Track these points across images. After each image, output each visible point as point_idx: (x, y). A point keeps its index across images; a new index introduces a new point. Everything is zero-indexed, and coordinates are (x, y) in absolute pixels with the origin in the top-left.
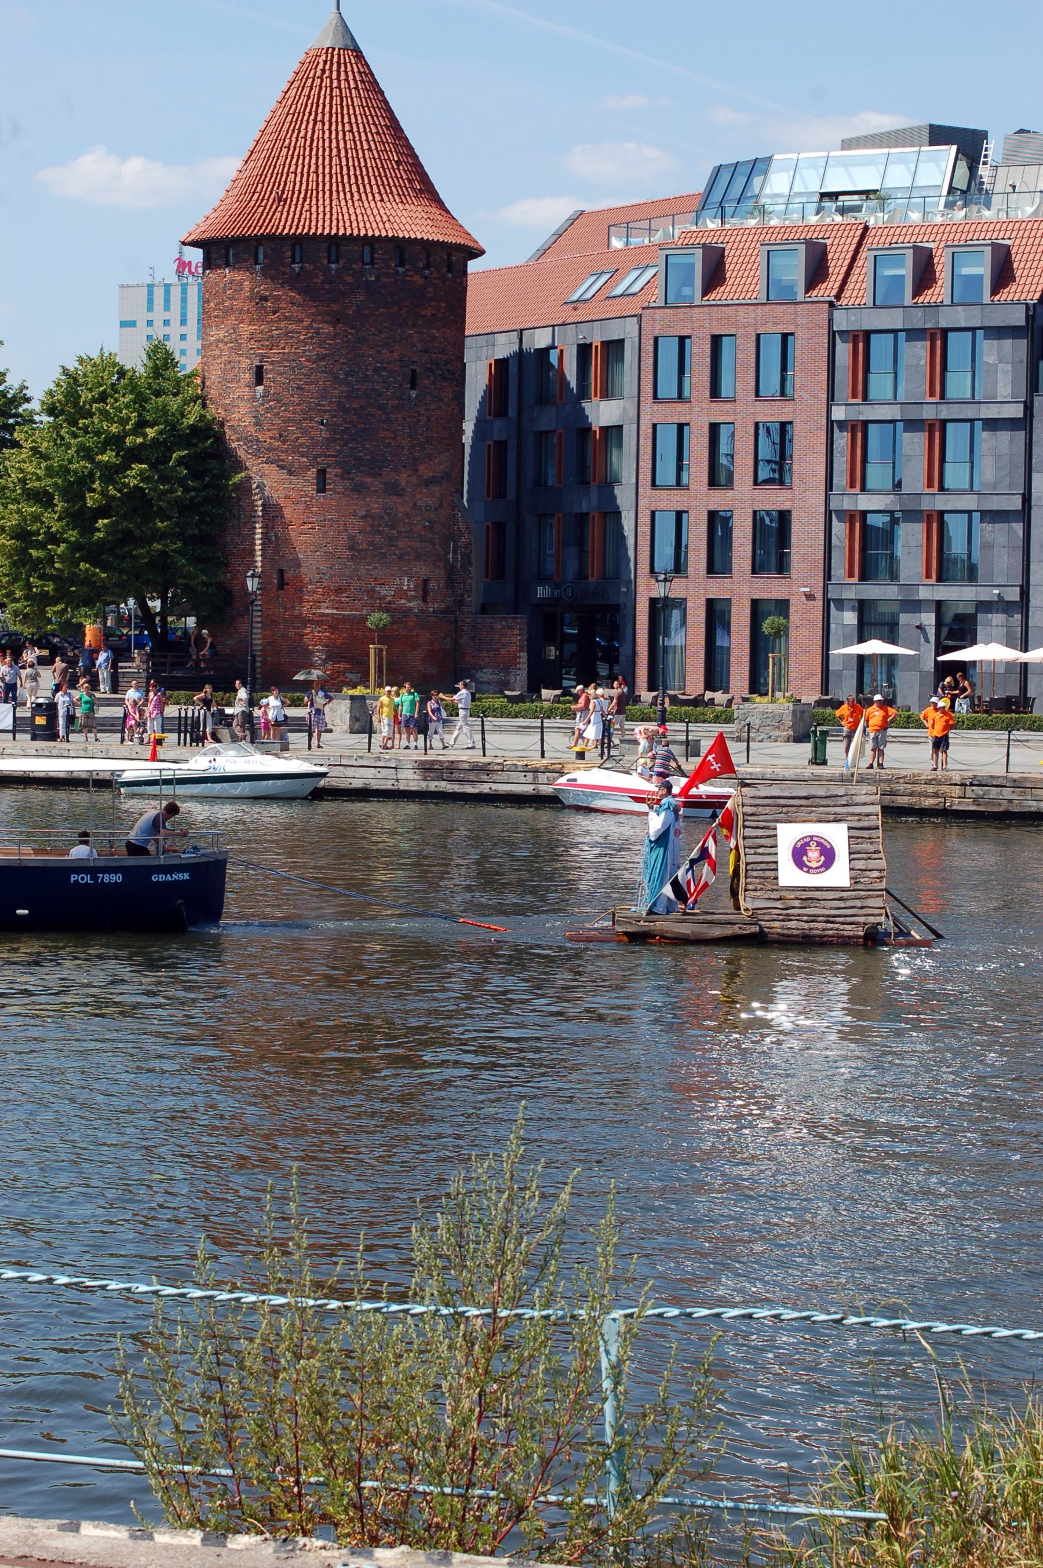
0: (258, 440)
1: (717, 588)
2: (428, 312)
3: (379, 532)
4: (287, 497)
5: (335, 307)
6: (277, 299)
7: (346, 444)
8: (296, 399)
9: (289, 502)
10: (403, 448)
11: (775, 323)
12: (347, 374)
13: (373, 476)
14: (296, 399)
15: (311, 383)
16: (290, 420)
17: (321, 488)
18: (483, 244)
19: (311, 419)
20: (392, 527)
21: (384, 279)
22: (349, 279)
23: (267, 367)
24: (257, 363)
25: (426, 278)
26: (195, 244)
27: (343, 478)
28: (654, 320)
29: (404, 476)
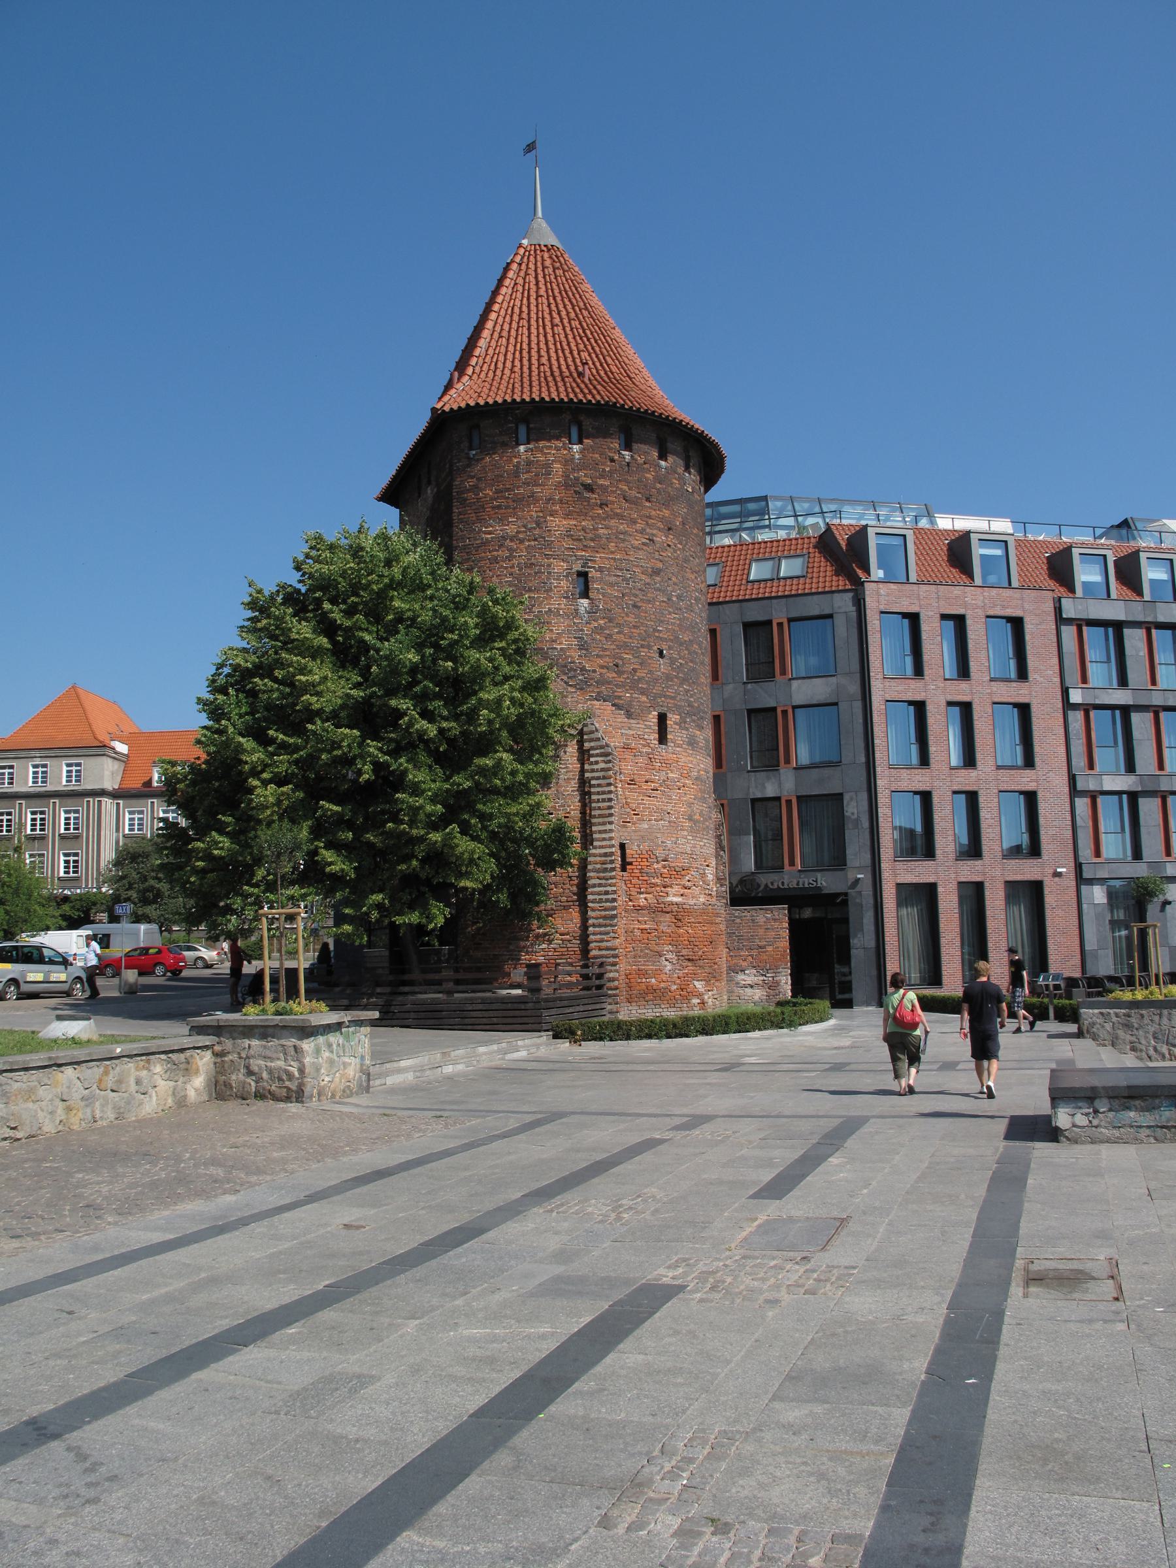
0: (583, 669)
1: (970, 871)
4: (627, 747)
5: (667, 513)
6: (604, 489)
7: (681, 684)
8: (631, 619)
9: (628, 755)
11: (1004, 607)
12: (679, 597)
14: (631, 619)
15: (649, 601)
16: (625, 646)
17: (663, 739)
19: (649, 647)
23: (593, 573)
24: (577, 567)
27: (679, 724)
28: (879, 594)
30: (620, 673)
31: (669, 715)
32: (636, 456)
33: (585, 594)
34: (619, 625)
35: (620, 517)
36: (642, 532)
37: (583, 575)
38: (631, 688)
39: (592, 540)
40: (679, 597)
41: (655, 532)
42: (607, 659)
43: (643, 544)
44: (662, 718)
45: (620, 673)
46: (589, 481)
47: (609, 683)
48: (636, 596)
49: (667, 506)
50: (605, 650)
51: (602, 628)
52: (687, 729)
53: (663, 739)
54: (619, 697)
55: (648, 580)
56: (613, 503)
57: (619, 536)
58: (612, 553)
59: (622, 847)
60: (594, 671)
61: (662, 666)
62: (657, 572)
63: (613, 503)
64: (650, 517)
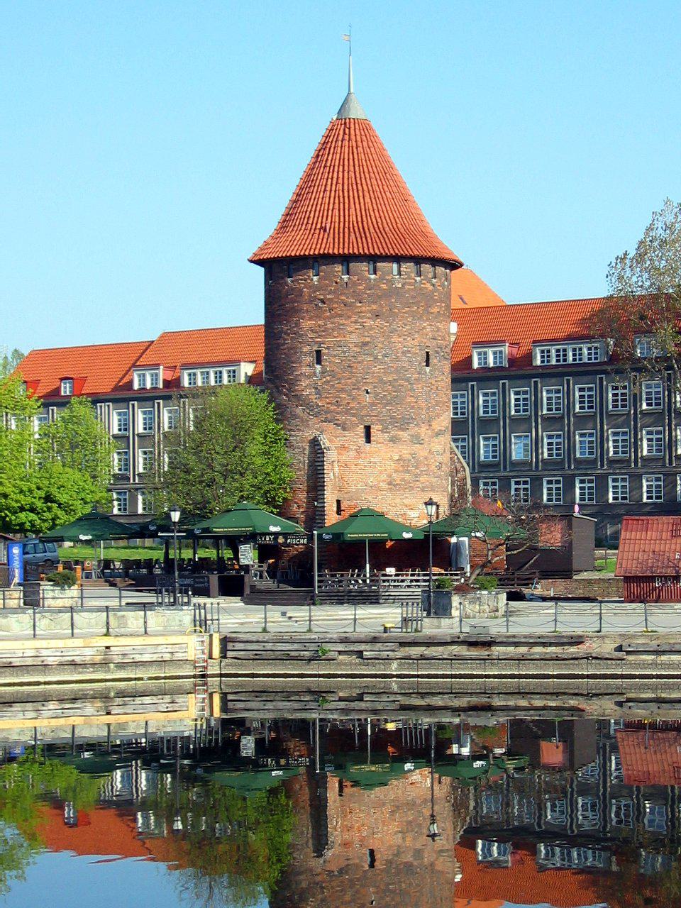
0: (318, 405)
2: (435, 310)
3: (408, 471)
5: (374, 307)
10: (422, 409)
13: (403, 430)
16: (343, 390)
17: (368, 440)
18: (462, 259)
19: (359, 389)
20: (417, 468)
21: (407, 287)
22: (384, 286)
23: (324, 351)
24: (315, 348)
25: (434, 285)
26: (259, 262)
29: (423, 429)
30: (338, 406)
31: (372, 426)
32: (351, 277)
33: (319, 362)
34: (339, 379)
35: (340, 316)
36: (356, 322)
37: (318, 352)
38: (346, 414)
39: (323, 331)
40: (384, 356)
41: (365, 320)
42: (331, 399)
43: (356, 329)
44: (368, 429)
45: (338, 406)
46: (322, 297)
47: (332, 412)
48: (350, 360)
49: (375, 303)
50: (330, 394)
51: (328, 382)
52: (389, 432)
53: (368, 440)
54: (338, 420)
55: (358, 351)
56: (336, 308)
57: (339, 327)
58: (335, 337)
59: (338, 502)
60: (323, 406)
61: (368, 398)
62: (365, 344)
63: (336, 308)
64: (361, 312)
